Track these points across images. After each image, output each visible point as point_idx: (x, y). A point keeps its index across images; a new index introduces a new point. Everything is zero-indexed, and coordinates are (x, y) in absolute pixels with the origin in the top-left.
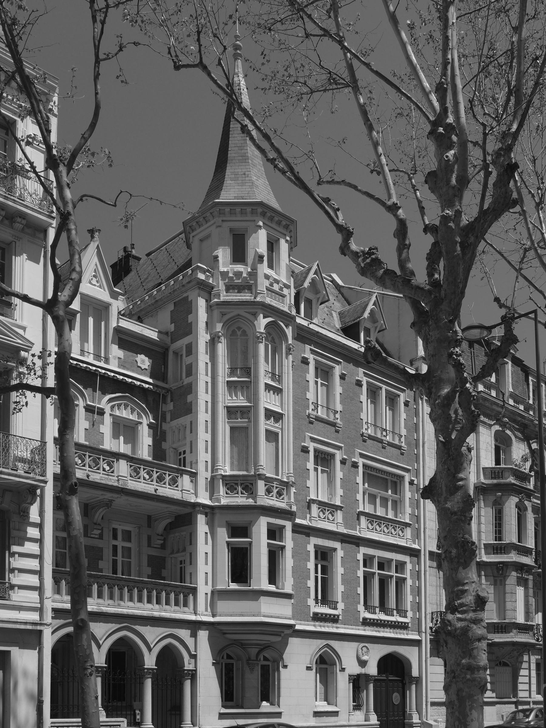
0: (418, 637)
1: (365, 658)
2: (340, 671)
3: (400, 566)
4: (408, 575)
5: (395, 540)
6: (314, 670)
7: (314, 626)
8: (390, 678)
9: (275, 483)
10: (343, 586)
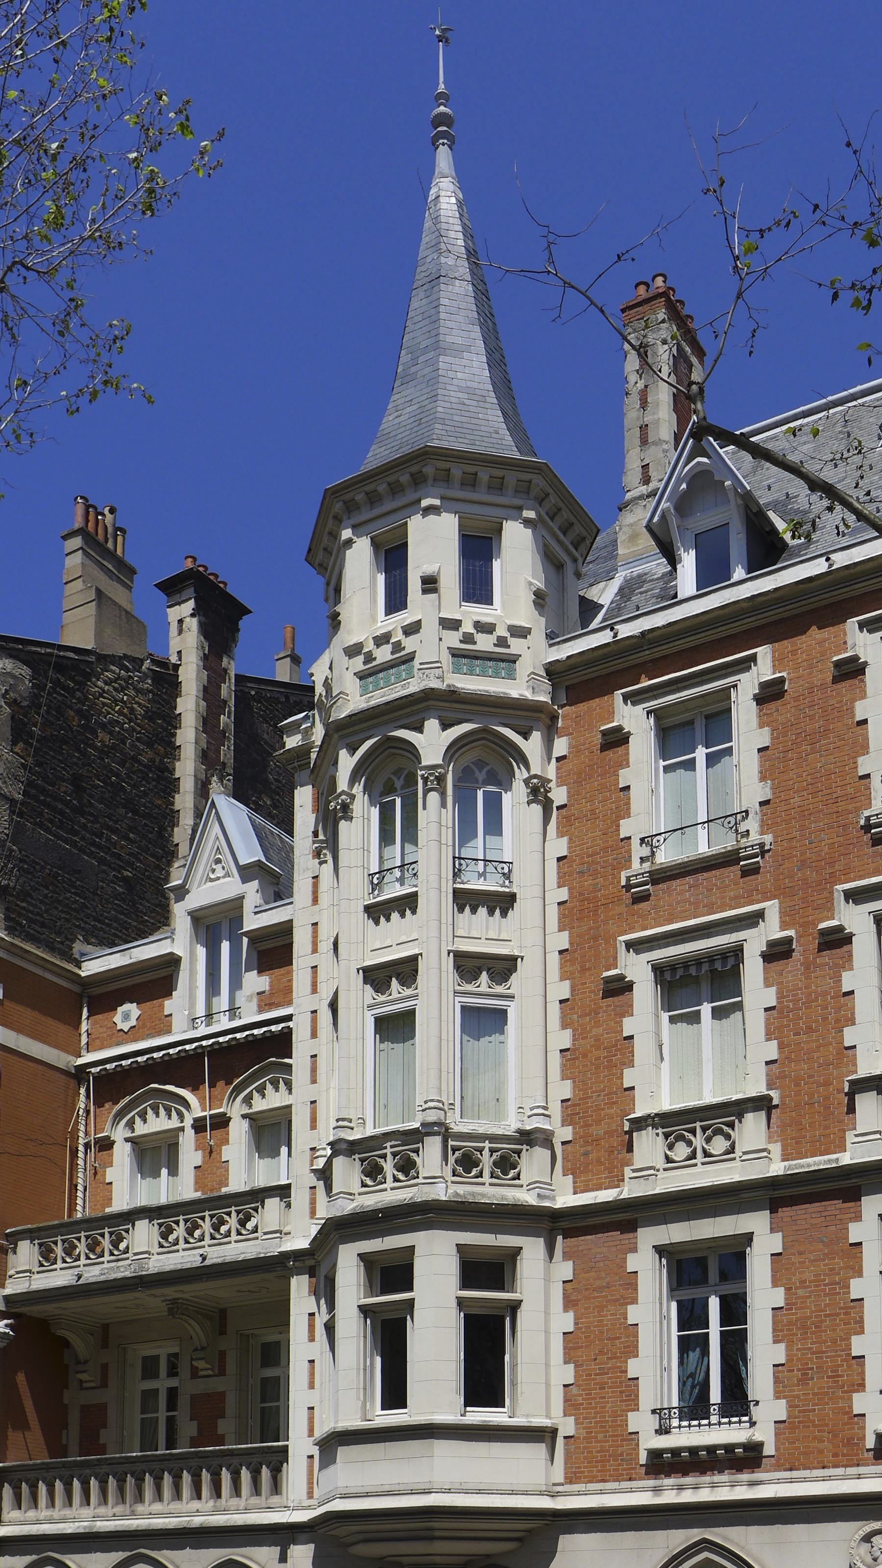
9: (388, 1144)
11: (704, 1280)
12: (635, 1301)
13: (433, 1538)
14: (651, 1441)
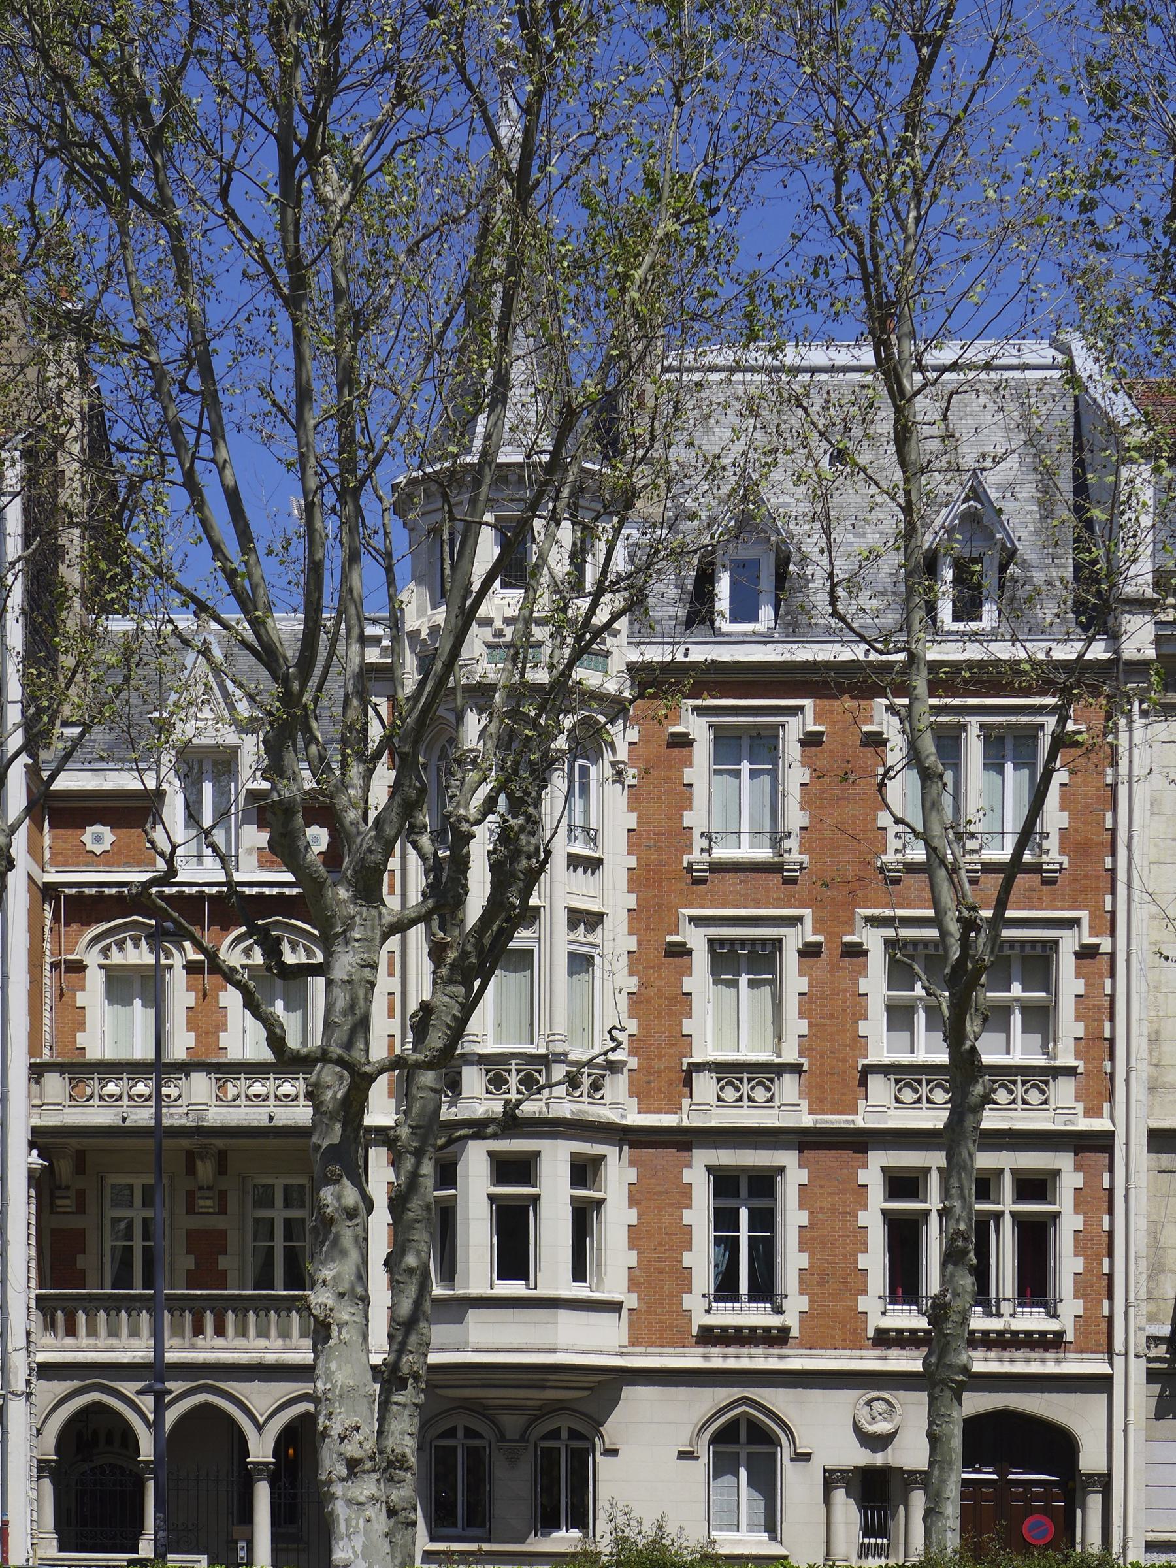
0: (1103, 1368)
1: (882, 1427)
2: (792, 1460)
3: (1035, 1186)
4: (1065, 1202)
5: (1003, 1118)
6: (704, 1460)
7: (706, 1357)
8: (1011, 1477)
10: (806, 1255)
11: (736, 1194)
12: (689, 1207)
13: (545, 1387)
14: (701, 1319)
